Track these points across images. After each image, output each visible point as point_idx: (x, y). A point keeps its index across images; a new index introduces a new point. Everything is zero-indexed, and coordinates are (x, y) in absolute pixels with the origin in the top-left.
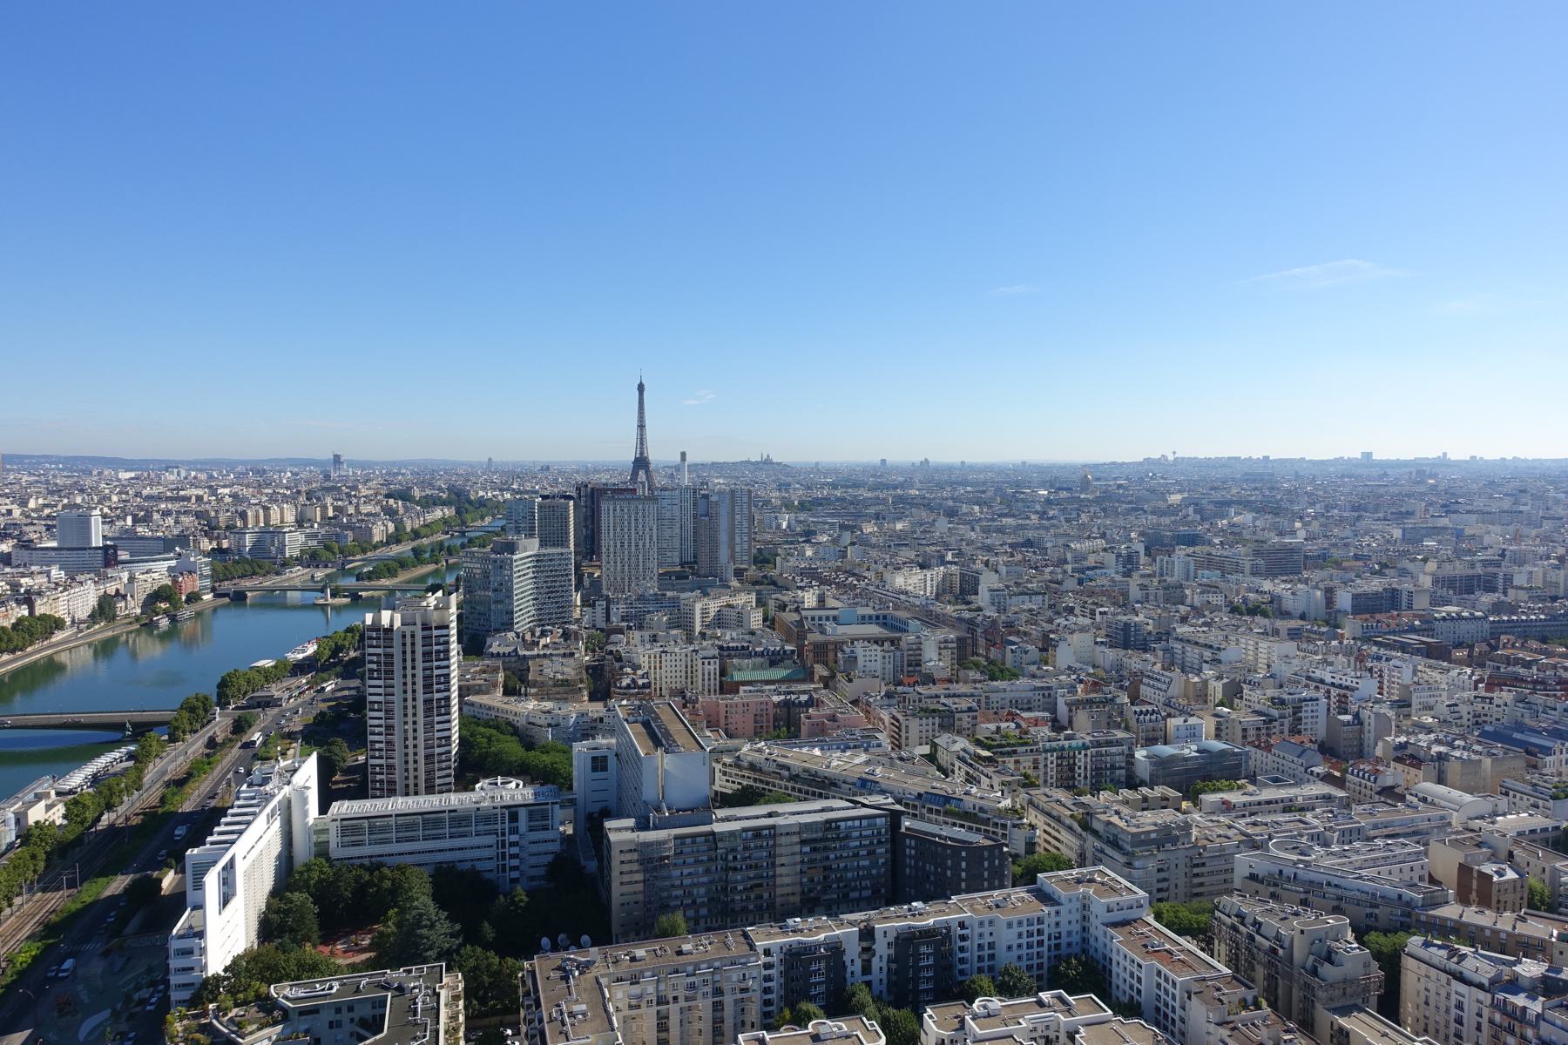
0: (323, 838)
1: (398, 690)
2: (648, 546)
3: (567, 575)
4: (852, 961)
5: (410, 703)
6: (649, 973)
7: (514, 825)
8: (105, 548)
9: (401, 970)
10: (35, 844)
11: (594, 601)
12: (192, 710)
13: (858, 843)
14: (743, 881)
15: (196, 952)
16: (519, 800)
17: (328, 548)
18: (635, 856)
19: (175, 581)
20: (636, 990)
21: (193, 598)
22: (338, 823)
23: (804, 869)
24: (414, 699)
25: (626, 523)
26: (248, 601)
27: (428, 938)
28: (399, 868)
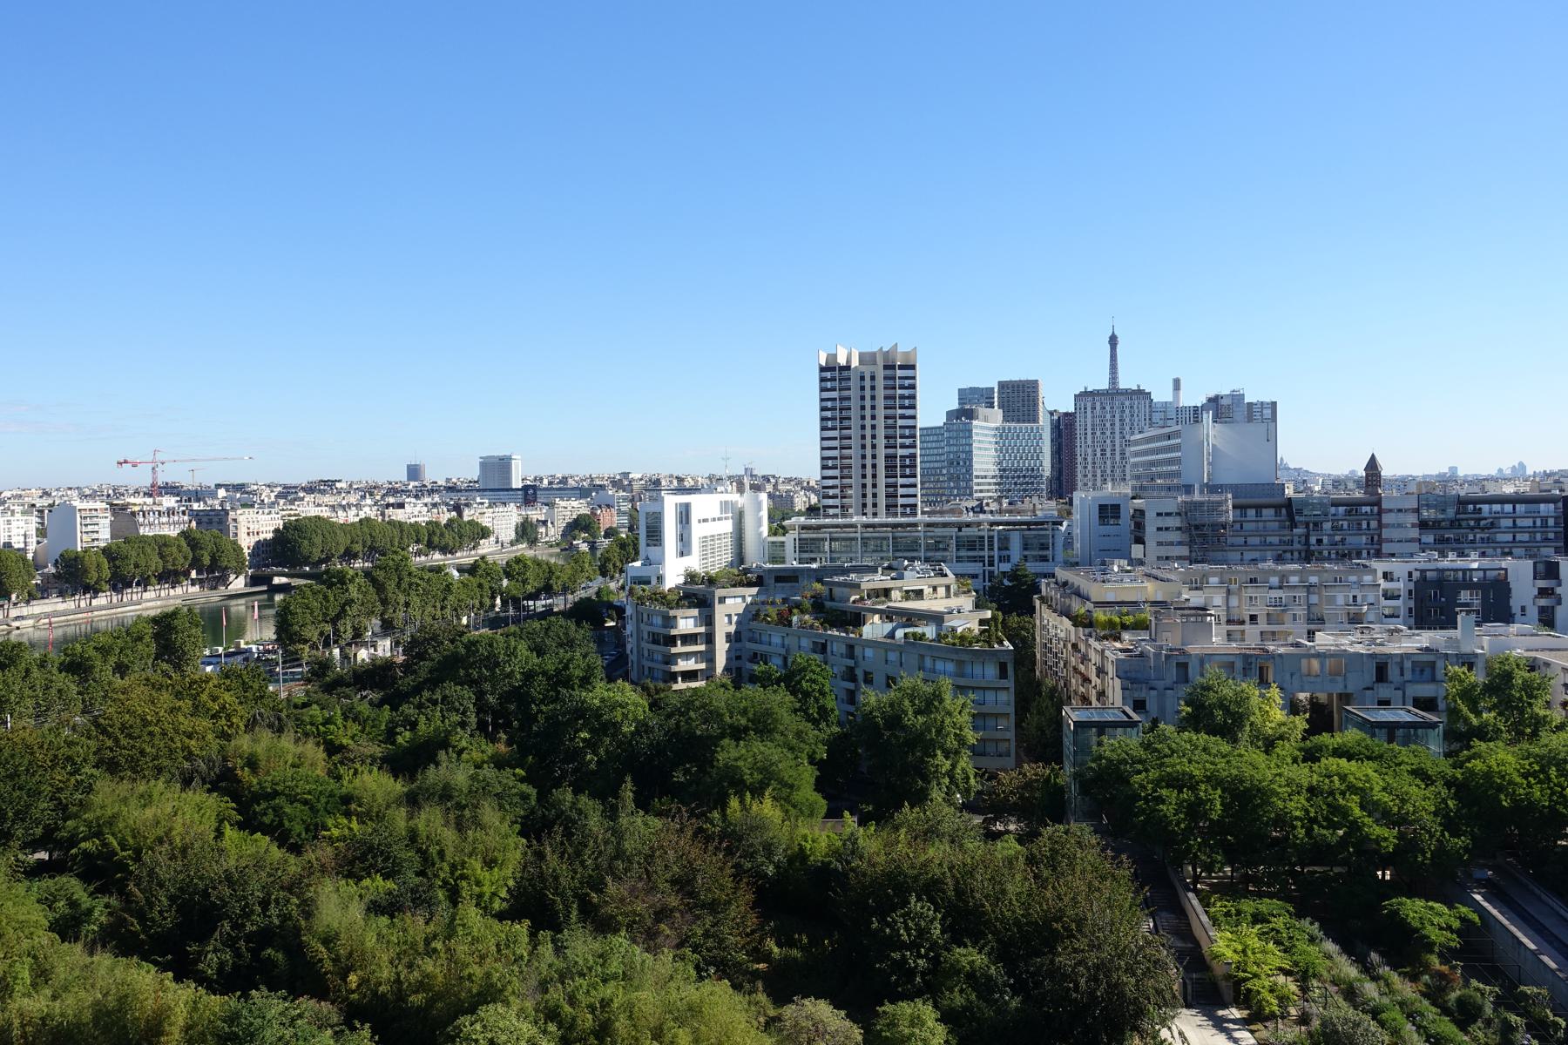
1: (855, 442)
4: (1523, 609)
7: (1005, 553)
8: (525, 488)
10: (481, 576)
13: (1509, 537)
18: (1174, 522)
25: (1108, 425)
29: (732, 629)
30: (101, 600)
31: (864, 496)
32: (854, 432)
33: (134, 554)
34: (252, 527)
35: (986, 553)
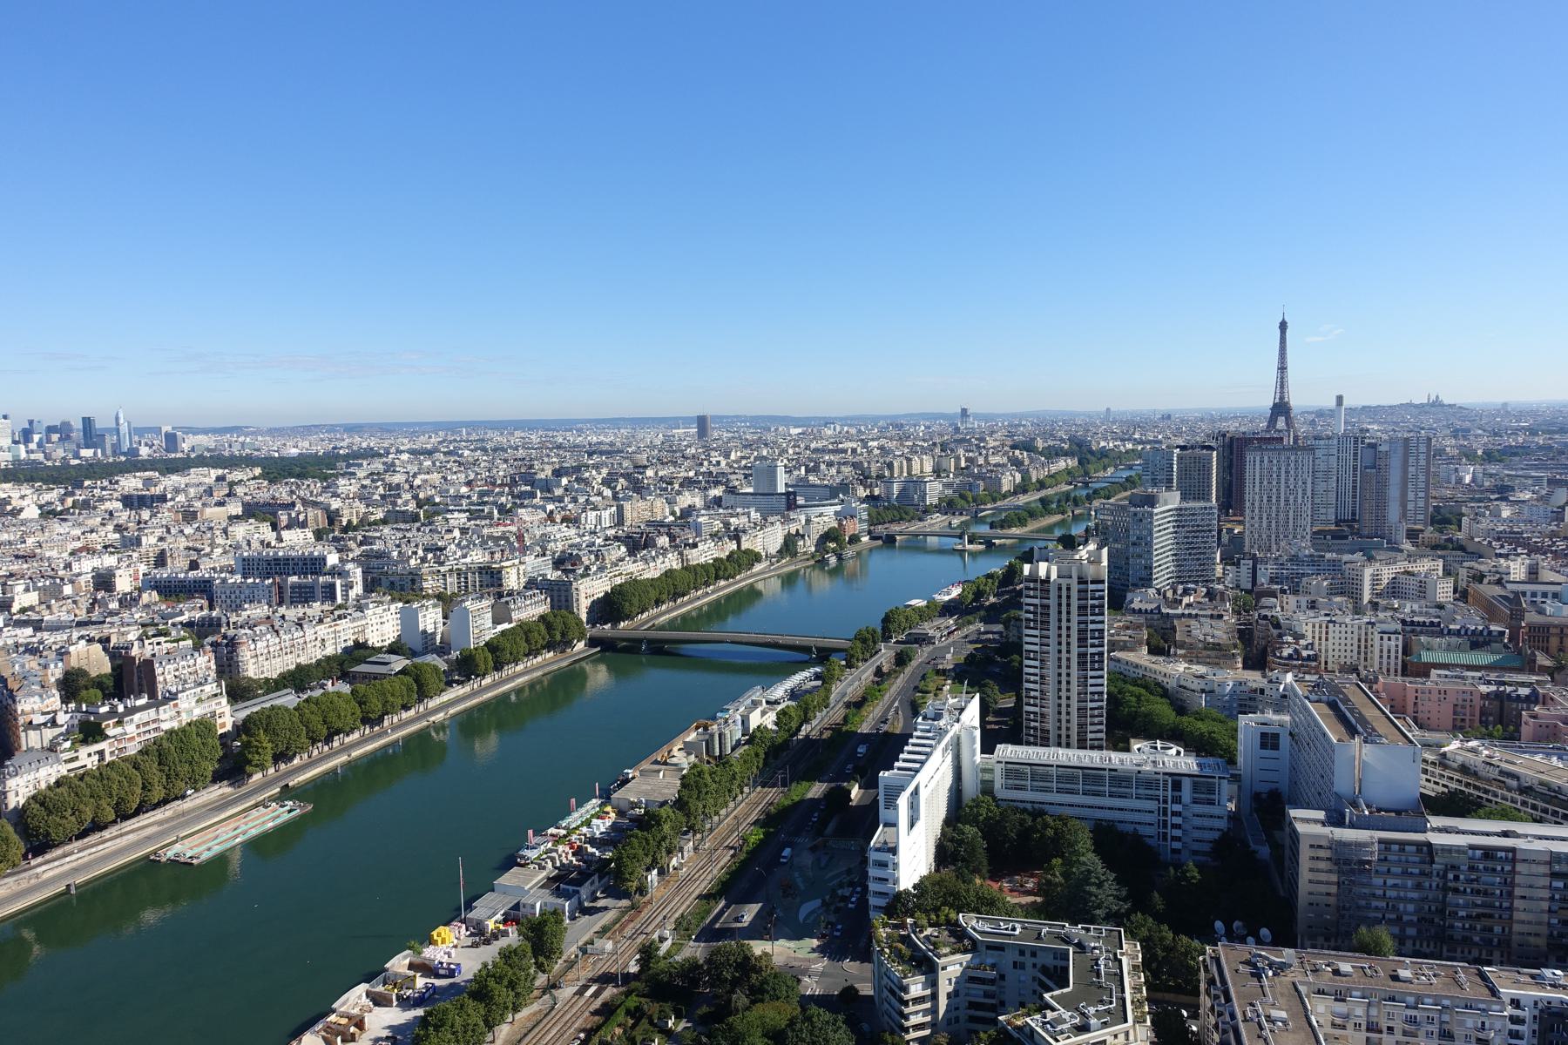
0: (987, 777)
1: (1053, 641)
2: (1300, 501)
3: (1210, 531)
5: (1064, 655)
6: (1358, 994)
7: (1177, 794)
8: (788, 494)
9: (1080, 926)
11: (1239, 560)
12: (864, 641)
14: (1466, 906)
15: (890, 866)
16: (1183, 769)
17: (962, 497)
18: (1327, 854)
19: (840, 524)
20: (1341, 1008)
21: (854, 539)
22: (1003, 765)
23: (1555, 908)
24: (1068, 652)
25: (1275, 476)
26: (897, 544)
27: (1096, 897)
28: (1060, 818)
29: (951, 989)
30: (488, 680)
31: (1060, 682)
32: (1053, 632)
33: (508, 645)
34: (588, 591)
35: (1161, 793)
